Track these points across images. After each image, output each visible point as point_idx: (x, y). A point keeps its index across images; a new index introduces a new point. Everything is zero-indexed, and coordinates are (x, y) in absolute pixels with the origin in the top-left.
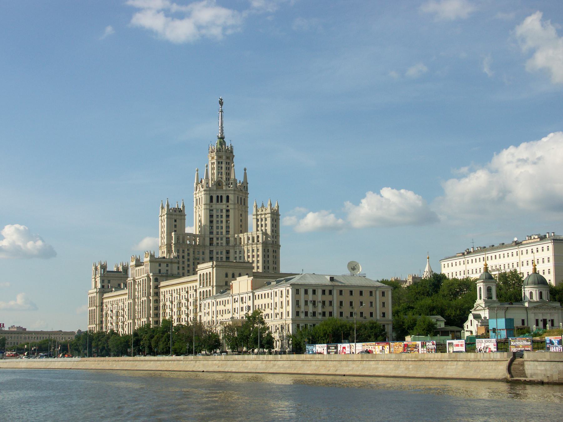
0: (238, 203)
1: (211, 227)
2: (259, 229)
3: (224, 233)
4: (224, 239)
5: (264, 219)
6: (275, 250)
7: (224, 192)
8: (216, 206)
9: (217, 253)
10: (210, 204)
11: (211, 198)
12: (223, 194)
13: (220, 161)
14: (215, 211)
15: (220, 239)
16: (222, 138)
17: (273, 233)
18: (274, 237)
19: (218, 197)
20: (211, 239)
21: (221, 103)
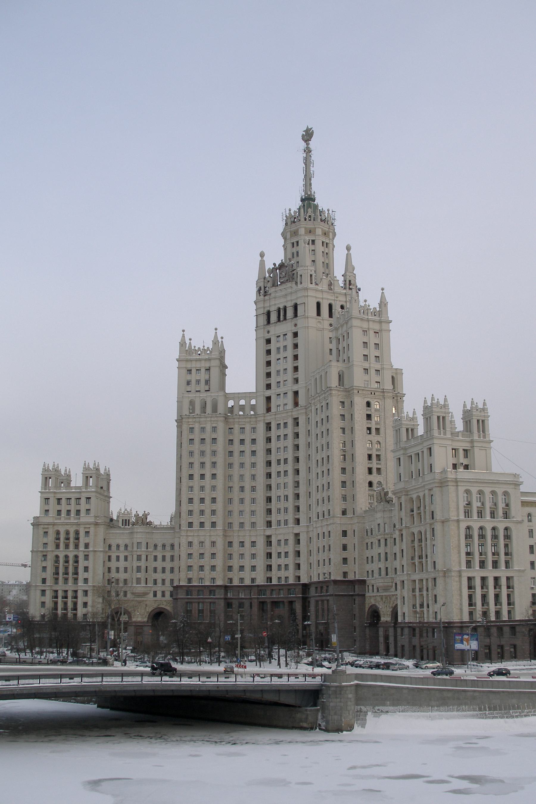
0: (319, 314)
4: (290, 395)
7: (289, 298)
10: (264, 328)
12: (287, 302)
13: (294, 240)
19: (279, 310)
20: (269, 399)
21: (308, 135)
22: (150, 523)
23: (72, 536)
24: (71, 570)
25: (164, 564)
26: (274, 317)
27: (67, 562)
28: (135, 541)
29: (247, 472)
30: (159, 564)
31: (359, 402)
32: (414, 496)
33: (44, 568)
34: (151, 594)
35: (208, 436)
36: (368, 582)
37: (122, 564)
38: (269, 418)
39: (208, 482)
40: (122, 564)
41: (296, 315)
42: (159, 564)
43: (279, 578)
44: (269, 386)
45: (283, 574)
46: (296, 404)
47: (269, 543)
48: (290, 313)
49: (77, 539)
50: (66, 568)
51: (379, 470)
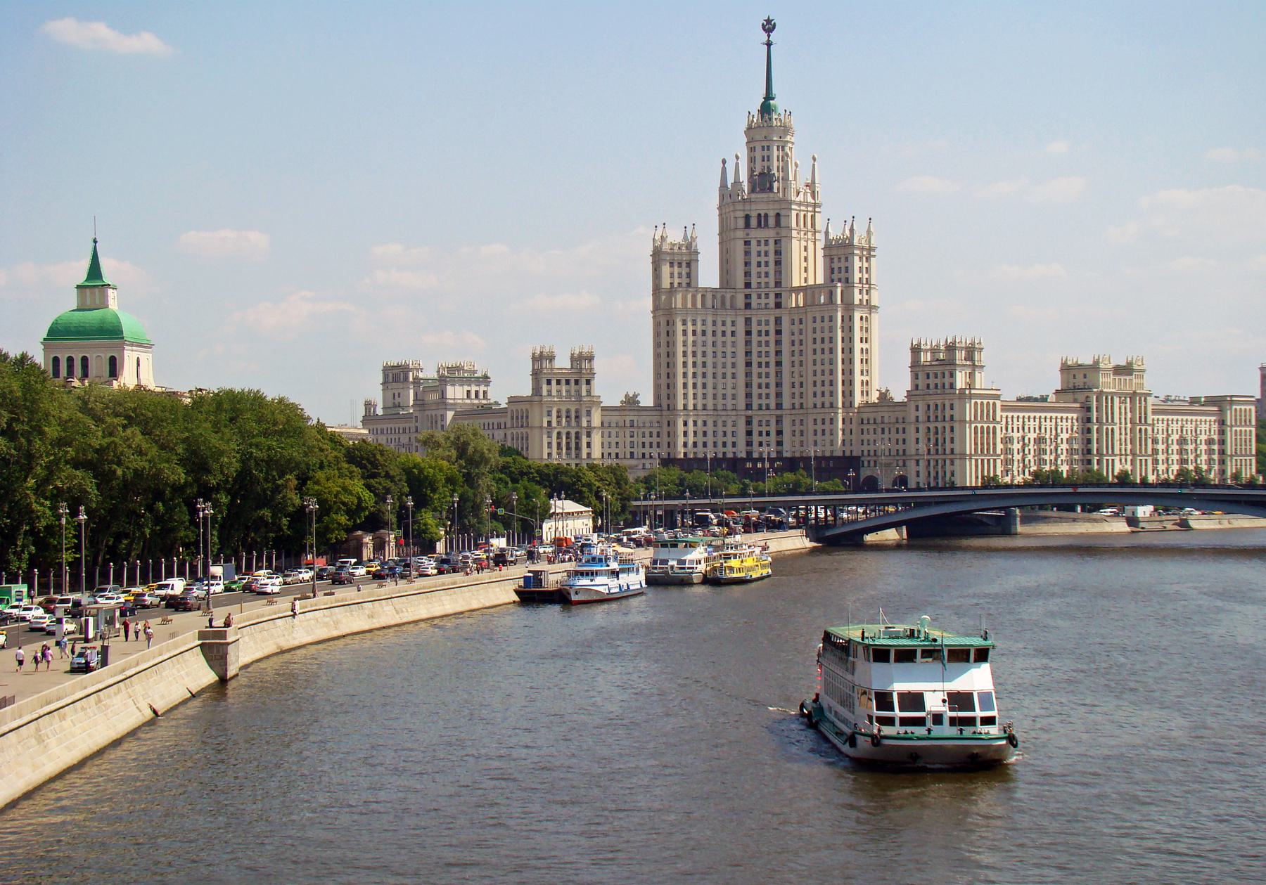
1: (747, 274)
2: (835, 276)
3: (772, 284)
4: (772, 296)
5: (843, 260)
6: (864, 316)
7: (771, 206)
8: (756, 234)
9: (759, 324)
11: (747, 218)
13: (765, 144)
14: (754, 243)
15: (763, 296)
16: (769, 96)
17: (861, 285)
20: (748, 296)
21: (769, 27)
22: (638, 402)
23: (573, 415)
24: (573, 445)
25: (651, 440)
26: (754, 222)
29: (729, 360)
30: (647, 440)
31: (857, 315)
33: (550, 445)
36: (862, 459)
38: (748, 312)
41: (778, 224)
42: (647, 440)
44: (748, 285)
46: (778, 305)
47: (749, 422)
48: (772, 221)
50: (568, 444)
51: (867, 371)
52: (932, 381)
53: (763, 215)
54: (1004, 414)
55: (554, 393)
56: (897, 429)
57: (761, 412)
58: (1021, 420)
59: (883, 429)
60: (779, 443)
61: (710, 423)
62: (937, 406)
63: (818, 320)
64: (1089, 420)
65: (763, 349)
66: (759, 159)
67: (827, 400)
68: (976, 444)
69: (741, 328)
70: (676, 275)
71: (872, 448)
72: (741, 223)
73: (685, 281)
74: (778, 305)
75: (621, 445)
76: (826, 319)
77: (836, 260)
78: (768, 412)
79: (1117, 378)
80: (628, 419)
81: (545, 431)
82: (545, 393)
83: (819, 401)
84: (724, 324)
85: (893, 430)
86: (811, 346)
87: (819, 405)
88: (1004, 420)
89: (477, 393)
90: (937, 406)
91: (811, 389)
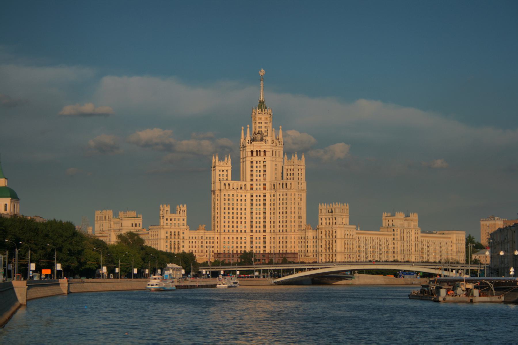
1: (252, 175)
4: (262, 185)
5: (292, 170)
7: (262, 147)
8: (255, 159)
9: (257, 196)
11: (252, 152)
13: (260, 121)
14: (255, 162)
15: (258, 184)
18: (300, 183)
20: (252, 185)
23: (177, 233)
24: (176, 246)
26: (255, 154)
27: (175, 244)
28: (206, 236)
32: (327, 231)
34: (205, 256)
35: (231, 197)
36: (299, 254)
37: (194, 244)
38: (252, 192)
39: (231, 215)
40: (194, 244)
41: (265, 154)
43: (256, 251)
44: (252, 180)
45: (258, 249)
46: (265, 189)
47: (252, 238)
48: (262, 153)
49: (179, 234)
50: (174, 246)
51: (301, 217)
52: (328, 221)
53: (258, 151)
54: (358, 236)
55: (169, 224)
56: (313, 241)
57: (257, 234)
58: (365, 239)
59: (307, 241)
60: (265, 247)
61: (235, 238)
62: (329, 231)
63: (281, 195)
64: (394, 239)
65: (258, 207)
66: (257, 127)
67: (285, 229)
68: (345, 248)
69: (249, 198)
70: (221, 175)
71: (303, 249)
72: (249, 154)
73: (225, 178)
74: (265, 189)
75: (197, 247)
76: (285, 195)
77: (289, 170)
78: (260, 234)
79: (406, 222)
80: (200, 236)
81: (165, 240)
82: (165, 224)
83: (281, 229)
84: (241, 196)
85: (312, 242)
86: (278, 206)
87: (281, 231)
88: (357, 238)
89: (136, 225)
90: (329, 231)
91: (278, 224)
